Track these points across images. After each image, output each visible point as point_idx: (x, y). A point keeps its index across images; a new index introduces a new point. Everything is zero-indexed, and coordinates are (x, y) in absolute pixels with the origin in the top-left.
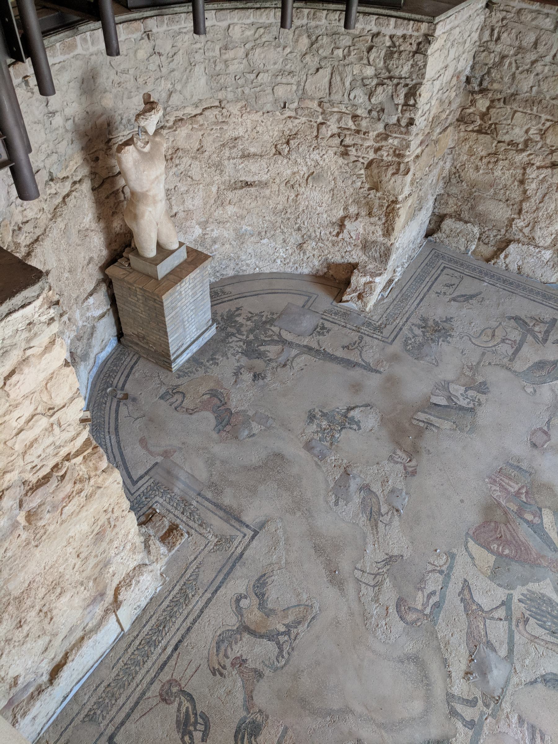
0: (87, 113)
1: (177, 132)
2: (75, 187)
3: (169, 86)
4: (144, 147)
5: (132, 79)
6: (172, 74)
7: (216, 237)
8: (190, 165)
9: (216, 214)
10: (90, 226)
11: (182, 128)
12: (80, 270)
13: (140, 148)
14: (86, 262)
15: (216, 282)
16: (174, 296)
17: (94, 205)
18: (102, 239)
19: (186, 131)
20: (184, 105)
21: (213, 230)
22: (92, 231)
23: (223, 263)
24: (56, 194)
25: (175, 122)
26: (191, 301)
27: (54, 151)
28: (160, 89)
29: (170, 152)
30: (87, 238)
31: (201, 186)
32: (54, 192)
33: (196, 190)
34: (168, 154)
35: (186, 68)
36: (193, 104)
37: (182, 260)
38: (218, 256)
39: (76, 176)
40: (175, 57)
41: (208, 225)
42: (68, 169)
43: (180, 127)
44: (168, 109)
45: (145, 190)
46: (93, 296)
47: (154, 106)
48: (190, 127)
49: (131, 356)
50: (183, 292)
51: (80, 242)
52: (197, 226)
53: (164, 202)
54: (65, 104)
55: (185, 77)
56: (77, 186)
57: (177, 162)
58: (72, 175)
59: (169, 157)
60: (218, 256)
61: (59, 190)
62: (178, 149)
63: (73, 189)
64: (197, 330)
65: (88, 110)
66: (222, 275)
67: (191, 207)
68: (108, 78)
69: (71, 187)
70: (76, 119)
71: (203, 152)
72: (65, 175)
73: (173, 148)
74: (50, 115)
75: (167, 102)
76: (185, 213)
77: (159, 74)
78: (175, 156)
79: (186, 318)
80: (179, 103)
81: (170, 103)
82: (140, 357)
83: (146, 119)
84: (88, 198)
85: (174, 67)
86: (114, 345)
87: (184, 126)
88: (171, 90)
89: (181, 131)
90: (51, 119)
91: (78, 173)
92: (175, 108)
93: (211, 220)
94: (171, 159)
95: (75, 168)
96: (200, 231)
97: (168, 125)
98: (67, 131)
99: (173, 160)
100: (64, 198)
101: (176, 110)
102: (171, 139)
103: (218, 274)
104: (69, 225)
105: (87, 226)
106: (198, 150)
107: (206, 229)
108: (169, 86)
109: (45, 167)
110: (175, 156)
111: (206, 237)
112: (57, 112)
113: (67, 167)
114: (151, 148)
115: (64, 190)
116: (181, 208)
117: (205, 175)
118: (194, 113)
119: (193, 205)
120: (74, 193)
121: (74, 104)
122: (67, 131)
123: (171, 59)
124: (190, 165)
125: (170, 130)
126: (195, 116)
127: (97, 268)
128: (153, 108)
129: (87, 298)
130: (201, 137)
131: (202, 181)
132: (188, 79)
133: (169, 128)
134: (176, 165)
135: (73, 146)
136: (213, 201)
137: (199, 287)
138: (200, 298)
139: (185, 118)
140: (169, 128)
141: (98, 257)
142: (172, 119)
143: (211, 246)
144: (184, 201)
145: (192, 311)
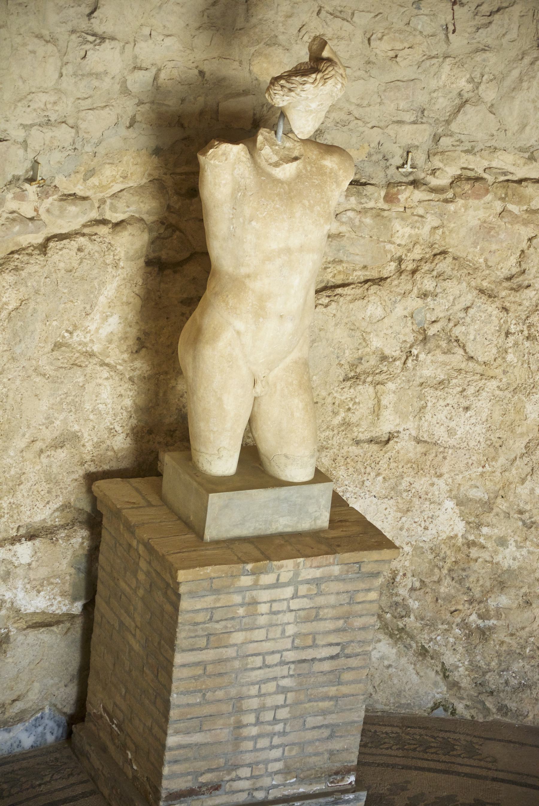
0: (202, 73)
1: (452, 207)
2: (95, 229)
3: (462, 83)
4: (276, 165)
5: (359, 38)
6: (479, 57)
7: (509, 571)
8: (467, 309)
9: (523, 491)
10: (105, 352)
11: (472, 202)
12: (21, 443)
13: (263, 164)
14: (48, 435)
15: (473, 723)
16: (224, 600)
17: (137, 302)
18: (128, 402)
19: (481, 214)
20: (493, 143)
21: (502, 542)
22: (103, 364)
23: (516, 667)
24: (32, 219)
25: (458, 179)
26: (291, 656)
27: (71, 122)
28: (433, 84)
29: (417, 254)
30: (79, 372)
31: (493, 384)
32: (31, 214)
33: (471, 390)
34: (411, 256)
35: (524, 54)
36: (521, 150)
37: (305, 525)
38: (502, 635)
39: (114, 208)
40: (497, 17)
41: (490, 518)
42: (94, 181)
43: (464, 195)
44: (445, 142)
45: (243, 271)
46: (37, 542)
47: (322, 66)
48: (498, 206)
49: (72, 780)
50: (263, 608)
51: (49, 370)
52: (450, 504)
53: (289, 326)
54: (146, 31)
55: (515, 73)
56: (103, 230)
57: (428, 284)
58: (103, 201)
59: (411, 266)
60: (502, 635)
61: (44, 216)
62: (444, 253)
63: (86, 231)
64: (287, 771)
65: (206, 68)
66: (502, 709)
67: (440, 433)
68: (289, 16)
69: (84, 226)
70: (163, 75)
71: (517, 289)
72: (80, 190)
73: (431, 246)
74: (91, 38)
75: (448, 122)
76: (420, 448)
77: (442, 48)
78: (426, 267)
79: (254, 703)
80: (480, 135)
81: (454, 127)
82: (92, 793)
83: (290, 90)
84: (122, 273)
85: (489, 41)
86: (50, 739)
87: (478, 197)
88: (466, 96)
89: (466, 207)
90: (88, 46)
91: (121, 205)
92: (467, 146)
93: (502, 505)
94: (414, 272)
95: (116, 188)
96: (460, 527)
97: (434, 182)
98: (125, 91)
99: (418, 276)
100: (48, 239)
101: (467, 151)
102: (432, 221)
103: (490, 703)
104: (32, 305)
105: (96, 348)
106: (509, 279)
107: (479, 526)
108: (462, 83)
109: (25, 144)
110: (426, 267)
111: (474, 552)
112: (113, 39)
113: (91, 173)
114: (299, 176)
115: (60, 222)
116: (411, 425)
117: (510, 357)
118: (520, 174)
119: (451, 432)
120: (82, 240)
121: (168, 41)
122: (125, 91)
123: (486, 20)
124: (467, 309)
125: (433, 196)
126: (520, 181)
127: (81, 472)
128: (315, 70)
129: (15, 540)
130: (524, 245)
131: (498, 372)
132: (521, 80)
133: (434, 190)
134: (424, 295)
135: (131, 134)
136: (519, 446)
137: (330, 625)
138: (326, 666)
139: (490, 179)
140: (434, 190)
141: (97, 446)
142: (453, 171)
143: (487, 593)
144: (424, 407)
145: (284, 690)
